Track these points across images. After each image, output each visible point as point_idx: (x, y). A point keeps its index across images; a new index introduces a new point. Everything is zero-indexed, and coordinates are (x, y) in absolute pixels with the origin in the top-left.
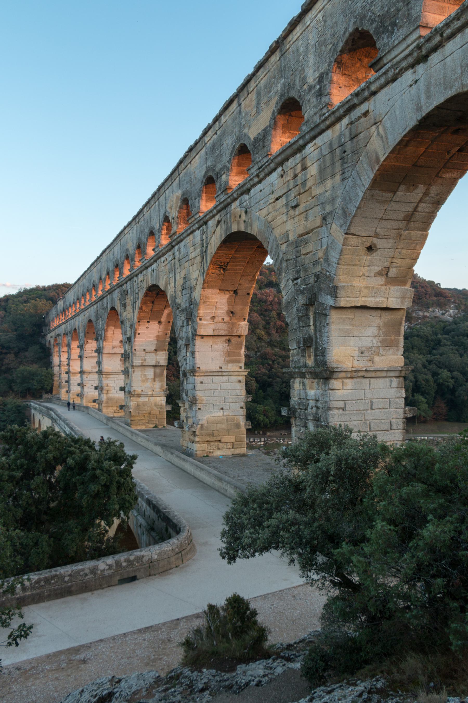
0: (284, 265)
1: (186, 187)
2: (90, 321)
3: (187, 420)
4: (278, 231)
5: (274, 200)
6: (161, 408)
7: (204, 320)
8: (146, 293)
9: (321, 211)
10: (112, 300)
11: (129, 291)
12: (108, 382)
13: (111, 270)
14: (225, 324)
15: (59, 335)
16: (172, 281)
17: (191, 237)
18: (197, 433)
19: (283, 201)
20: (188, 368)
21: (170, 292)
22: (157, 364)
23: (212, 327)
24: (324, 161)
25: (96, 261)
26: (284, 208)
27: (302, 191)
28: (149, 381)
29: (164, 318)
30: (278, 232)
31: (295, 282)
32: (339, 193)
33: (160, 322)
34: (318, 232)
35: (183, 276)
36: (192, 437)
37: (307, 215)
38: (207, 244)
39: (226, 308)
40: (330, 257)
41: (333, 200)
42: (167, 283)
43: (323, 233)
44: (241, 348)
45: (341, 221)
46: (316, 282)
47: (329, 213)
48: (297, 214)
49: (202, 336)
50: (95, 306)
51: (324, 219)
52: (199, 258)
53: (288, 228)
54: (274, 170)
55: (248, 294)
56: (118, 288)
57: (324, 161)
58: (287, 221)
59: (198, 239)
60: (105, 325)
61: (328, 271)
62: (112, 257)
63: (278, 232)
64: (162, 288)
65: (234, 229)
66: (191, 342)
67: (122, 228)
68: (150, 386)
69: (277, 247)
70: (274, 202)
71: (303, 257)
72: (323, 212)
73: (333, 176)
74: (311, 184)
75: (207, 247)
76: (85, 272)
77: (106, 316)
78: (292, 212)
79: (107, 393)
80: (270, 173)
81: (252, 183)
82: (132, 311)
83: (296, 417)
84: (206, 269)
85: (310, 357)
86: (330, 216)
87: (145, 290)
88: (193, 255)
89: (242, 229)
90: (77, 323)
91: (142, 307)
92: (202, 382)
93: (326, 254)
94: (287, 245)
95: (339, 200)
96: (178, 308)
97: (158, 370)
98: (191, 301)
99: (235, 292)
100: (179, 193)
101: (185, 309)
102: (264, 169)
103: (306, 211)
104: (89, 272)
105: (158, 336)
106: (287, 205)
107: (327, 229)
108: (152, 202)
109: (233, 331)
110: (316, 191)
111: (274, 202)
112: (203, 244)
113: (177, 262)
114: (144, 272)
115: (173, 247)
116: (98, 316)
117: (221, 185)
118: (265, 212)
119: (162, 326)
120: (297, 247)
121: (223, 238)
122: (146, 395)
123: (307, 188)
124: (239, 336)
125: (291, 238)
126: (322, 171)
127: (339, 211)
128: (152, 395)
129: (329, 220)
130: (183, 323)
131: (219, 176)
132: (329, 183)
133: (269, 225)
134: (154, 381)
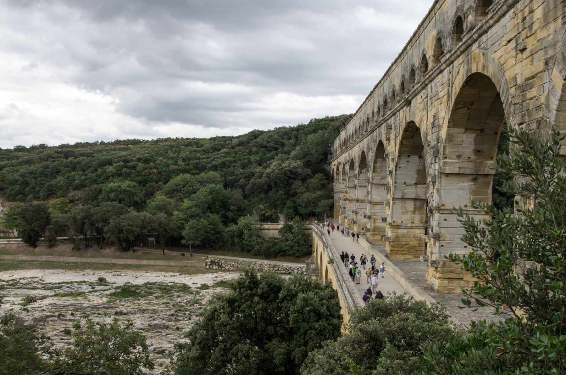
0: (512, 109)
1: (440, 26)
2: (363, 152)
3: (431, 256)
4: (508, 74)
5: (506, 42)
6: (420, 240)
7: (450, 158)
8: (406, 128)
9: (544, 56)
10: (380, 133)
11: (393, 125)
14: (471, 163)
15: (340, 163)
16: (425, 118)
17: (440, 76)
18: (438, 269)
19: (513, 44)
20: (434, 205)
21: (423, 130)
22: (417, 197)
23: (458, 165)
24: (548, 4)
25: (370, 95)
26: (514, 51)
27: (529, 34)
28: (409, 213)
30: (509, 75)
31: (521, 126)
32: (560, 37)
34: (541, 77)
36: (435, 273)
37: (532, 58)
38: (452, 84)
39: (472, 147)
40: (550, 103)
41: (554, 45)
42: (421, 120)
43: (545, 78)
44: (488, 188)
45: (561, 66)
46: (538, 128)
47: (550, 58)
48: (524, 58)
49: (447, 175)
50: (367, 138)
51: (546, 63)
52: (446, 98)
53: (517, 72)
54: (507, 12)
55: (496, 133)
56: (384, 122)
57: (548, 4)
58: (516, 64)
59: (446, 79)
61: (548, 118)
62: (382, 92)
63: (509, 75)
64: (417, 124)
65: (474, 70)
66: (437, 180)
67: (390, 65)
68: (410, 218)
69: (508, 90)
70: (506, 44)
71: (528, 101)
72: (546, 57)
73: (555, 20)
74: (537, 27)
75: (452, 87)
76: (362, 105)
78: (520, 55)
79: (374, 222)
80: (504, 15)
81: (488, 25)
83: (516, 265)
84: (451, 108)
85: (530, 204)
86: (551, 61)
88: (441, 94)
89: (480, 71)
90: (354, 154)
92: (445, 220)
93: (547, 99)
94: (516, 89)
95: (559, 45)
96: (429, 145)
97: (418, 204)
98: (438, 139)
99: (482, 130)
100: (434, 33)
101: (433, 147)
102: (497, 12)
103: (532, 55)
104: (364, 105)
106: (516, 48)
107: (549, 75)
108: (414, 41)
109: (480, 169)
110: (541, 34)
111: (506, 44)
112: (449, 84)
113: (429, 100)
115: (426, 85)
116: (369, 148)
117: (467, 26)
118: (498, 54)
120: (523, 91)
121: (465, 78)
122: (406, 227)
123: (533, 32)
124: (487, 175)
125: (519, 82)
126: (546, 14)
127: (559, 56)
128: (411, 227)
129: (551, 65)
130: (432, 160)
131: (466, 16)
132: (552, 26)
133: (501, 68)
134: (414, 214)
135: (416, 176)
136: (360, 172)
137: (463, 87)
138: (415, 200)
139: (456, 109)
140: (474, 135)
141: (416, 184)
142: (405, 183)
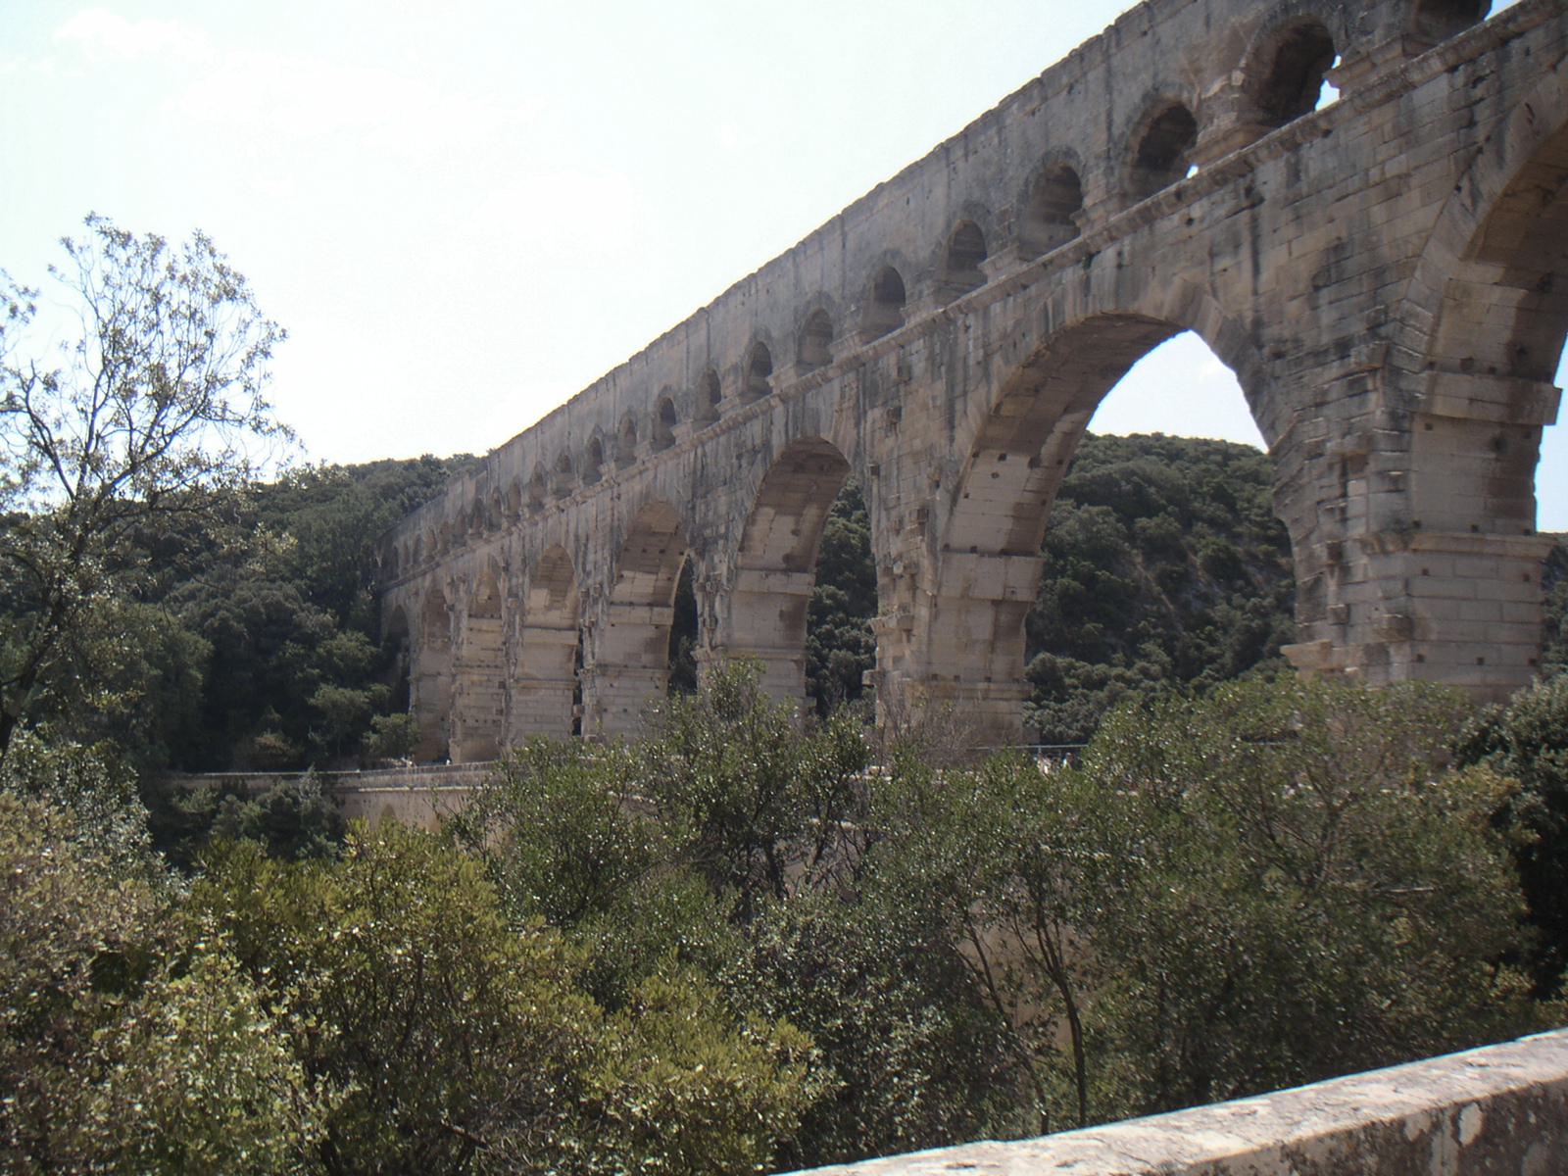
7: (1445, 369)
8: (1037, 354)
13: (775, 334)
22: (1008, 595)
29: (1049, 448)
33: (1034, 463)
35: (1313, 242)
39: (1506, 336)
60: (749, 505)
77: (759, 471)
87: (1033, 342)
91: (998, 406)
92: (1425, 572)
105: (1019, 506)
114: (1033, 290)
119: (1038, 473)
135: (1008, 525)
138: (996, 603)
140: (1517, 294)
141: (1005, 553)
142: (974, 550)
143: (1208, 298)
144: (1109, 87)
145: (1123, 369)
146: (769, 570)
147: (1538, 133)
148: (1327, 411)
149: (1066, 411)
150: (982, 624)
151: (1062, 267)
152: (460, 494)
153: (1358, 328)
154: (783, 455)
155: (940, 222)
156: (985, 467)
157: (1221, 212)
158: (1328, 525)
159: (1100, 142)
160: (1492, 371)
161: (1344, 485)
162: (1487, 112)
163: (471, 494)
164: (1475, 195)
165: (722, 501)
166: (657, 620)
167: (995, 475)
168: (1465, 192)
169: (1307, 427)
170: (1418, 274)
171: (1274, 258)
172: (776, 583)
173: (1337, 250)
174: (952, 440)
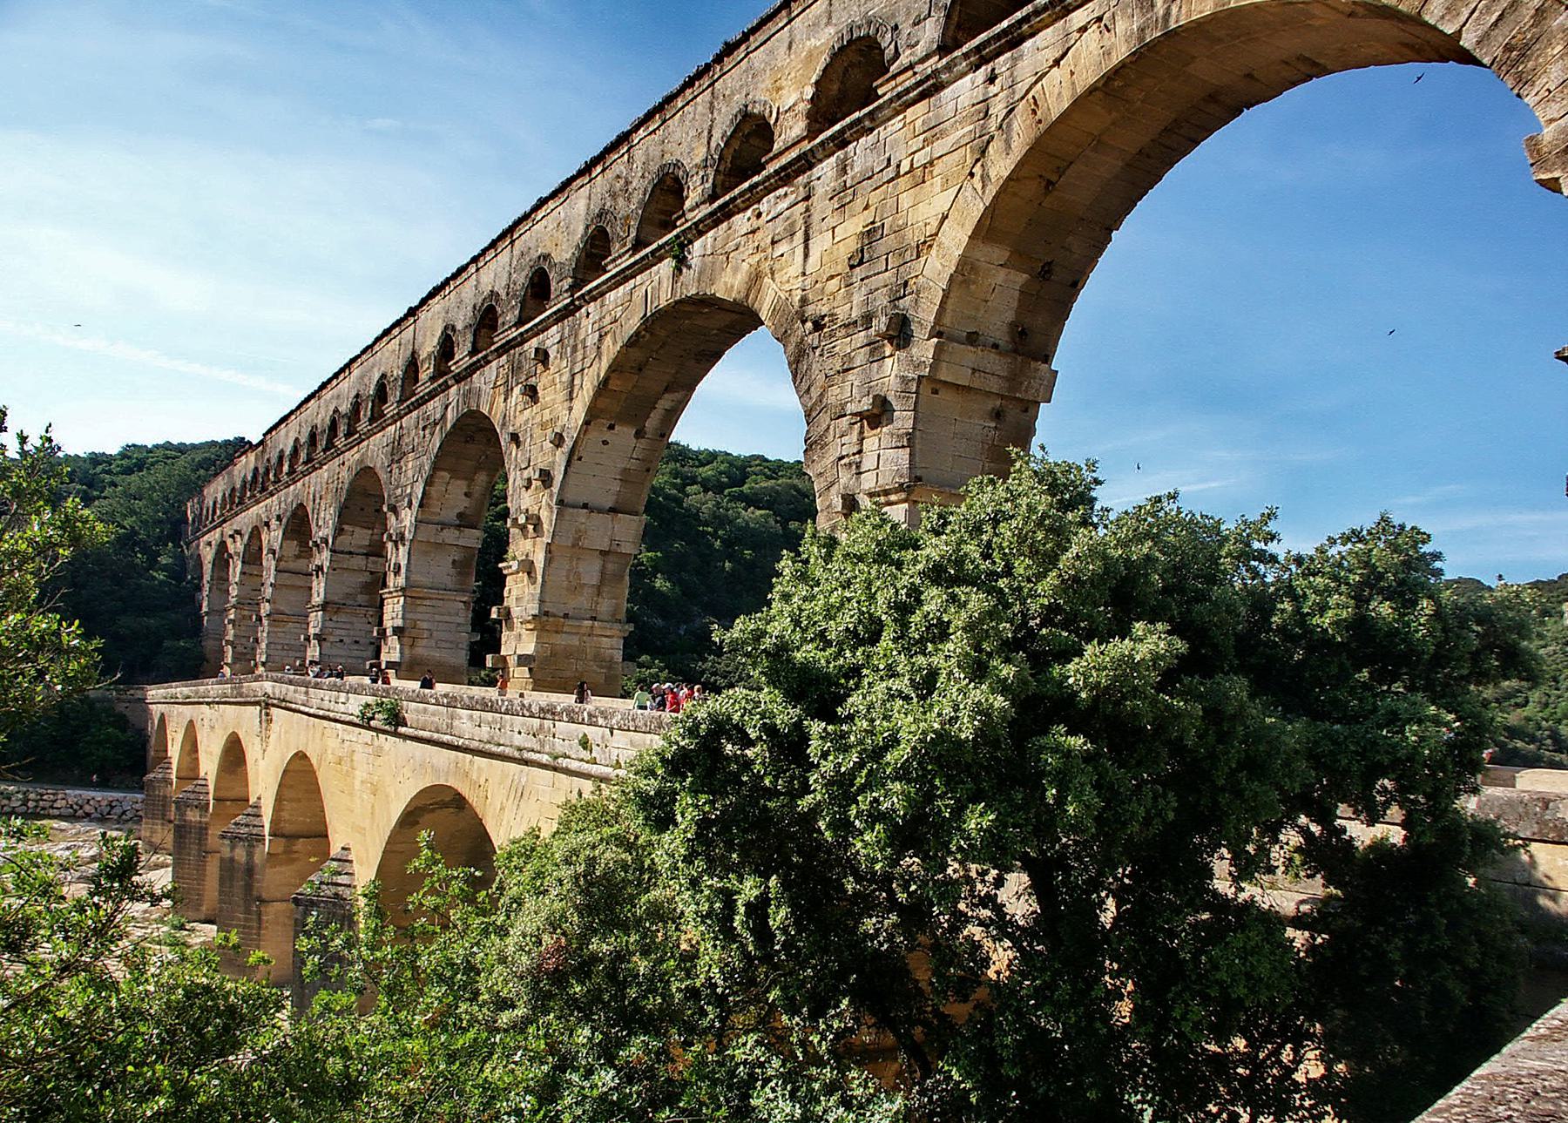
7: (951, 339)
8: (637, 333)
12: (419, 616)
13: (459, 327)
15: (238, 532)
29: (652, 423)
33: (639, 434)
39: (1010, 316)
68: (587, 605)
82: (562, 395)
87: (633, 323)
116: (397, 452)
119: (643, 443)
135: (616, 487)
136: (339, 531)
137: (1092, 90)
138: (603, 553)
139: (1018, 180)
140: (1024, 277)
141: (613, 510)
142: (585, 506)
143: (767, 280)
144: (712, 109)
145: (718, 356)
146: (444, 525)
147: (1040, 121)
148: (851, 376)
149: (666, 390)
150: (590, 571)
151: (661, 259)
152: (246, 465)
153: (882, 300)
154: (453, 426)
155: (581, 229)
156: (595, 435)
157: (784, 205)
158: (845, 478)
159: (701, 153)
160: (995, 346)
161: (861, 440)
162: (1001, 106)
163: (252, 466)
164: (985, 179)
165: (410, 464)
166: (371, 567)
167: (605, 443)
168: (977, 177)
169: (835, 390)
170: (934, 252)
171: (819, 244)
172: (450, 536)
173: (871, 234)
174: (571, 409)
